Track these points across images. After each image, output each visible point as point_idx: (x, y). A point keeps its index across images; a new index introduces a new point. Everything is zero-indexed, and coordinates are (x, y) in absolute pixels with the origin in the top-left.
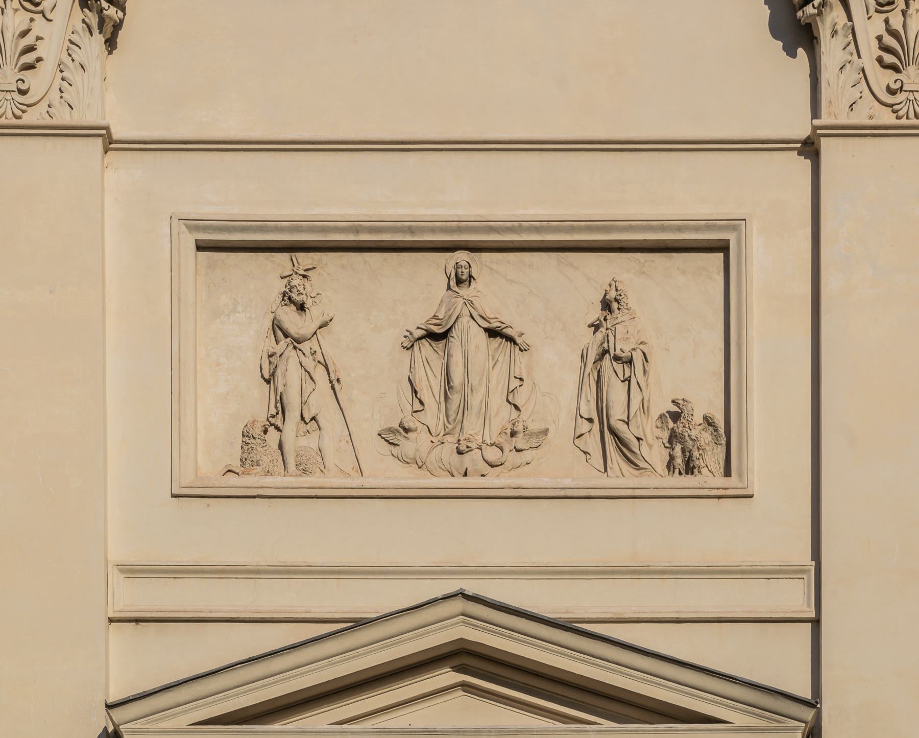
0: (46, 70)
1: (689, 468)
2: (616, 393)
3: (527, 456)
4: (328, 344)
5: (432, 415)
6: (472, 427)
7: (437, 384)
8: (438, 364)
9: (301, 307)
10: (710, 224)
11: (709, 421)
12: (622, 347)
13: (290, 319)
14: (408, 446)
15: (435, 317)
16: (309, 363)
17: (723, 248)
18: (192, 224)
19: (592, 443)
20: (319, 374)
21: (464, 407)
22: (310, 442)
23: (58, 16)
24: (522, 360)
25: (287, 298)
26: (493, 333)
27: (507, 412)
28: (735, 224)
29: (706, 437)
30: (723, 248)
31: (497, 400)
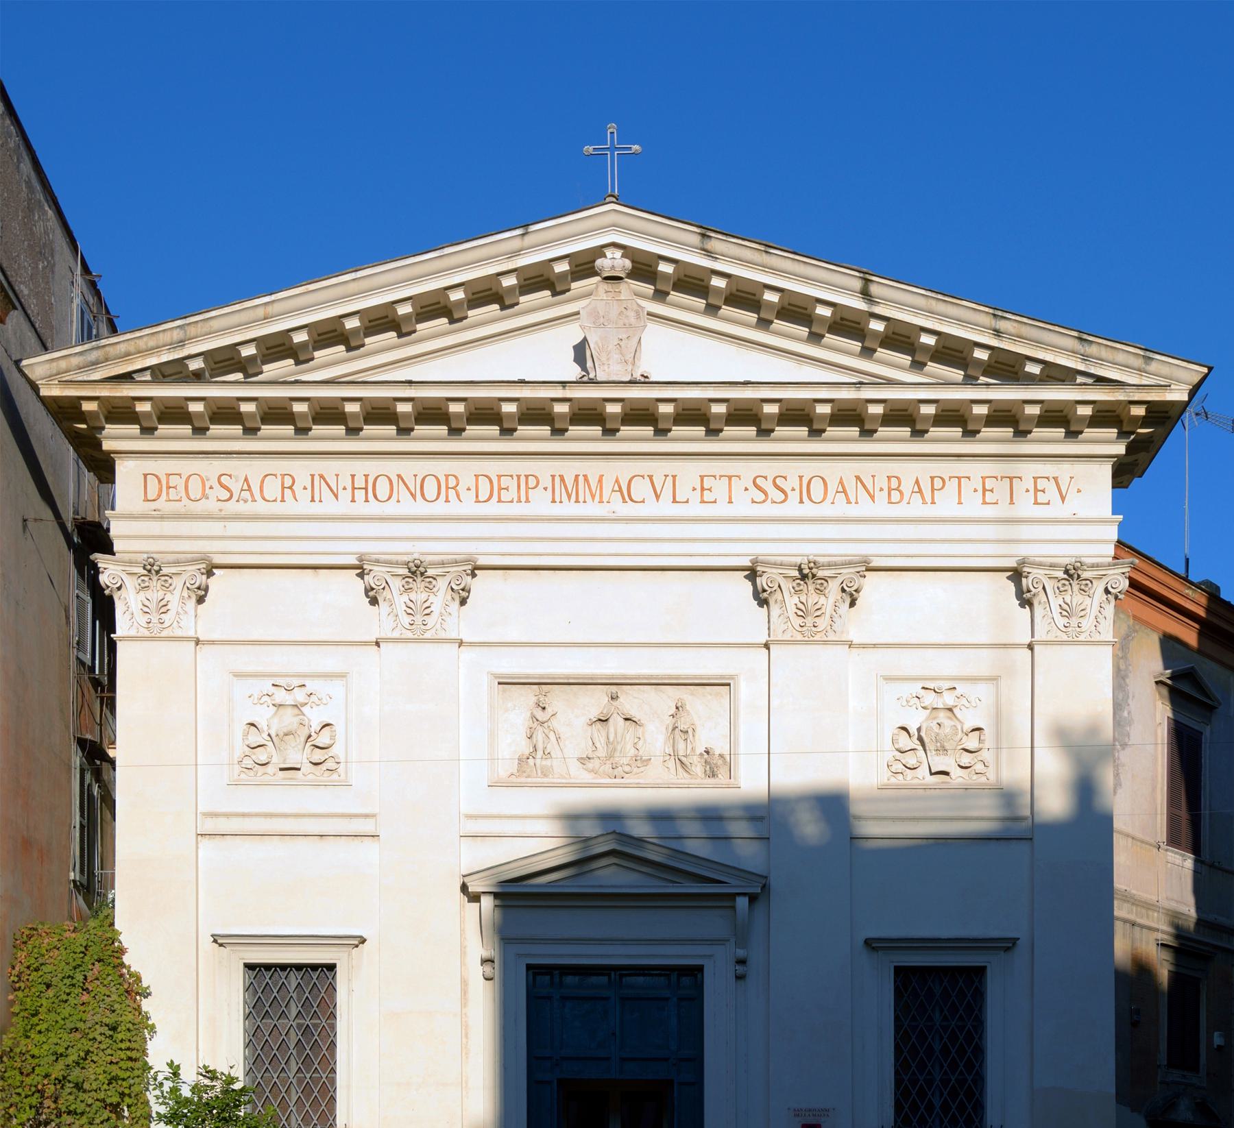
0: (435, 616)
1: (713, 775)
2: (681, 746)
3: (642, 769)
7: (603, 740)
8: (604, 733)
10: (722, 677)
11: (721, 756)
12: (682, 727)
13: (541, 715)
15: (602, 713)
18: (496, 676)
19: (671, 764)
20: (552, 735)
21: (615, 750)
22: (548, 763)
23: (441, 594)
24: (640, 730)
26: (626, 719)
28: (732, 677)
29: (720, 762)
30: (729, 685)
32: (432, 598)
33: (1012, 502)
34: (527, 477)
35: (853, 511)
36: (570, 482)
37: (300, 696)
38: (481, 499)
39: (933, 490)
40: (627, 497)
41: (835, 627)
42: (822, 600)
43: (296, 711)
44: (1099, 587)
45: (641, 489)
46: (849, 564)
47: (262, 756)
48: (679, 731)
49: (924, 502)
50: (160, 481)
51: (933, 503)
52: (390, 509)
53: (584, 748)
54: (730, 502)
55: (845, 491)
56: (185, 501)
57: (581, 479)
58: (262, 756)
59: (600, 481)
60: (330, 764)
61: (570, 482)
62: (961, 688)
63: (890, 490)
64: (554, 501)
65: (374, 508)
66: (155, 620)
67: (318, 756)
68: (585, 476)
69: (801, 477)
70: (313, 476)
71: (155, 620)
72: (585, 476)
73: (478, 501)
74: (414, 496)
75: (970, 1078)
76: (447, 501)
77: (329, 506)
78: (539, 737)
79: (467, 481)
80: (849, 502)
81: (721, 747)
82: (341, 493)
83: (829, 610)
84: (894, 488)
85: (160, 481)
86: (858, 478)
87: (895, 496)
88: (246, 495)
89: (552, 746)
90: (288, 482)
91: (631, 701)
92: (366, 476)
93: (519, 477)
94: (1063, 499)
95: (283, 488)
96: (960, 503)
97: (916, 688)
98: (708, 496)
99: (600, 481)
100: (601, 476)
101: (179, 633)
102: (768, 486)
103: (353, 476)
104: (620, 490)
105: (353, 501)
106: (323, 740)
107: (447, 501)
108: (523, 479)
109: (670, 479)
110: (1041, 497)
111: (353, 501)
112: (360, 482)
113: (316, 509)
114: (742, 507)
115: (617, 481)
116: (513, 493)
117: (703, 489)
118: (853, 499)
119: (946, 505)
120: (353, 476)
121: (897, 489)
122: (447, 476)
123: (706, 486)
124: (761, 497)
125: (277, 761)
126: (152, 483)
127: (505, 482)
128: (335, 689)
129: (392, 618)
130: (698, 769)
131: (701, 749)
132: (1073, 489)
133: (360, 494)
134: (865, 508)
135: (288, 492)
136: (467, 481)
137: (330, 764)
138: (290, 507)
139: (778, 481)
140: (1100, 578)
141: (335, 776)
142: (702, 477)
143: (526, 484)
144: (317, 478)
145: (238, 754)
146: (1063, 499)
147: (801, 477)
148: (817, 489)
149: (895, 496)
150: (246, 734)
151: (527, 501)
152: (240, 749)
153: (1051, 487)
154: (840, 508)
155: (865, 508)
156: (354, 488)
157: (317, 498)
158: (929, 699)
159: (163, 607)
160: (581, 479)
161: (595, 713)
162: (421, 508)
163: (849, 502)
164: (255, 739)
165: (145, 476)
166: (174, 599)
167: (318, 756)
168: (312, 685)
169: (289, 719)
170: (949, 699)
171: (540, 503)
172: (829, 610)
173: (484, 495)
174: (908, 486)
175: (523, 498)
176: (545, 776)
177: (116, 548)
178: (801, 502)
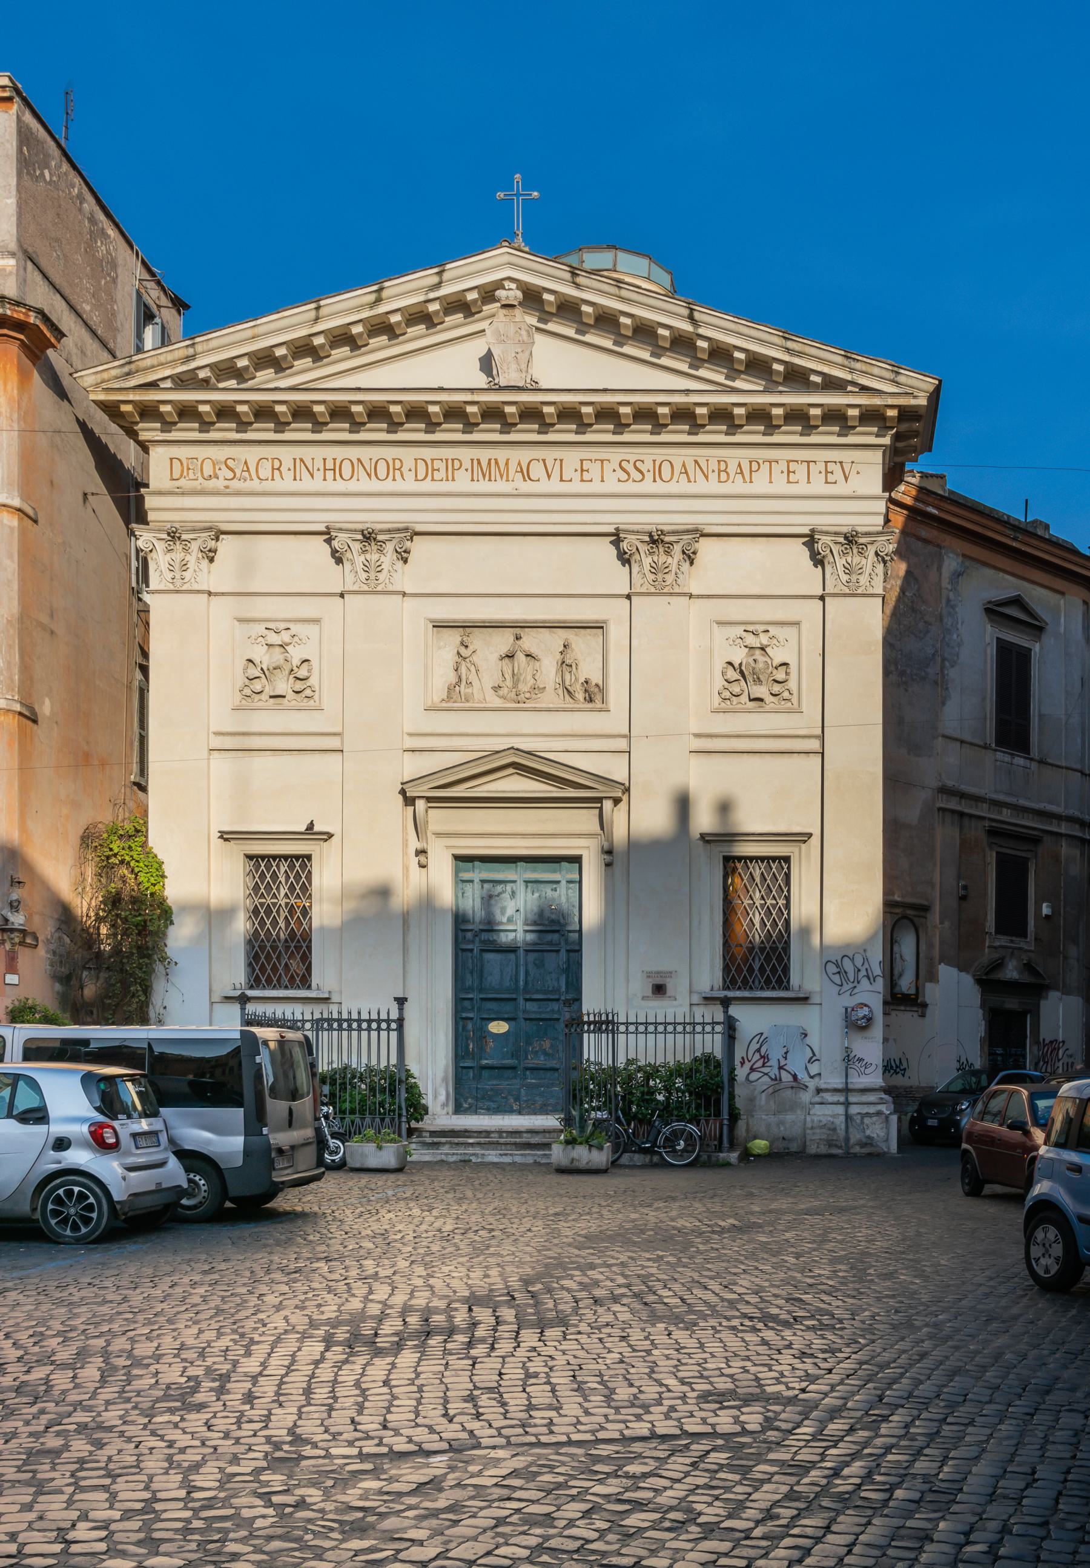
0: (385, 572)
1: (591, 700)
2: (567, 677)
4: (475, 658)
5: (509, 682)
6: (523, 687)
7: (510, 672)
8: (510, 666)
9: (467, 647)
10: (597, 622)
11: (597, 685)
12: (568, 662)
13: (463, 651)
14: (501, 693)
16: (469, 665)
17: (602, 627)
19: (560, 692)
20: (473, 669)
21: (518, 680)
22: (469, 690)
23: (389, 555)
24: (537, 664)
25: (462, 643)
26: (527, 655)
27: (532, 681)
28: (605, 622)
29: (597, 690)
30: (602, 627)
31: (529, 677)
32: (383, 558)
33: (809, 482)
34: (453, 460)
35: (692, 489)
36: (484, 464)
37: (285, 637)
38: (419, 477)
39: (751, 471)
40: (527, 476)
41: (679, 582)
42: (670, 560)
43: (282, 650)
44: (871, 551)
45: (537, 470)
46: (687, 532)
47: (257, 686)
48: (565, 665)
49: (745, 482)
50: (182, 464)
51: (751, 482)
52: (352, 486)
53: (496, 679)
54: (602, 481)
55: (686, 473)
56: (201, 480)
57: (493, 462)
58: (257, 686)
59: (507, 464)
60: (308, 692)
61: (484, 464)
62: (773, 630)
63: (720, 471)
64: (473, 480)
65: (340, 486)
66: (178, 576)
67: (299, 686)
68: (496, 460)
69: (654, 461)
70: (295, 459)
71: (178, 576)
72: (496, 460)
73: (417, 480)
74: (369, 475)
75: (780, 946)
76: (394, 480)
77: (307, 484)
78: (463, 670)
79: (409, 463)
80: (689, 481)
81: (596, 678)
82: (316, 473)
83: (674, 568)
84: (722, 470)
85: (182, 464)
86: (696, 462)
87: (723, 476)
88: (246, 474)
89: (473, 677)
90: (277, 464)
91: (531, 641)
92: (334, 459)
93: (447, 460)
94: (846, 479)
95: (273, 469)
96: (771, 482)
97: (739, 630)
98: (586, 476)
99: (507, 464)
100: (508, 460)
101: (196, 587)
102: (630, 467)
103: (325, 460)
104: (522, 471)
105: (325, 479)
106: (302, 673)
107: (394, 480)
108: (450, 462)
109: (558, 462)
110: (831, 478)
111: (325, 479)
112: (329, 465)
113: (297, 486)
114: (612, 485)
115: (519, 464)
116: (442, 474)
117: (582, 470)
118: (692, 479)
119: (760, 484)
120: (325, 460)
121: (725, 471)
122: (394, 460)
123: (585, 468)
124: (624, 476)
125: (269, 691)
126: (176, 463)
127: (437, 464)
128: (312, 630)
129: (353, 574)
130: (580, 696)
131: (582, 680)
132: (854, 471)
133: (330, 474)
134: (701, 486)
135: (276, 472)
136: (409, 463)
137: (308, 692)
138: (279, 485)
139: (638, 464)
140: (872, 543)
141: (311, 702)
142: (582, 461)
143: (453, 466)
144: (298, 461)
145: (239, 684)
146: (846, 479)
147: (654, 461)
148: (666, 469)
149: (723, 476)
150: (245, 669)
151: (453, 480)
152: (241, 680)
153: (837, 468)
154: (683, 487)
155: (701, 486)
156: (325, 469)
157: (298, 478)
158: (751, 640)
159: (184, 567)
160: (493, 462)
161: (504, 650)
162: (374, 485)
163: (689, 481)
164: (254, 672)
165: (171, 459)
166: (192, 559)
167: (299, 686)
168: (295, 628)
169: (277, 656)
170: (764, 639)
171: (463, 482)
172: (674, 568)
173: (421, 475)
174: (732, 468)
175: (450, 478)
176: (468, 701)
177: (149, 518)
178: (655, 481)
